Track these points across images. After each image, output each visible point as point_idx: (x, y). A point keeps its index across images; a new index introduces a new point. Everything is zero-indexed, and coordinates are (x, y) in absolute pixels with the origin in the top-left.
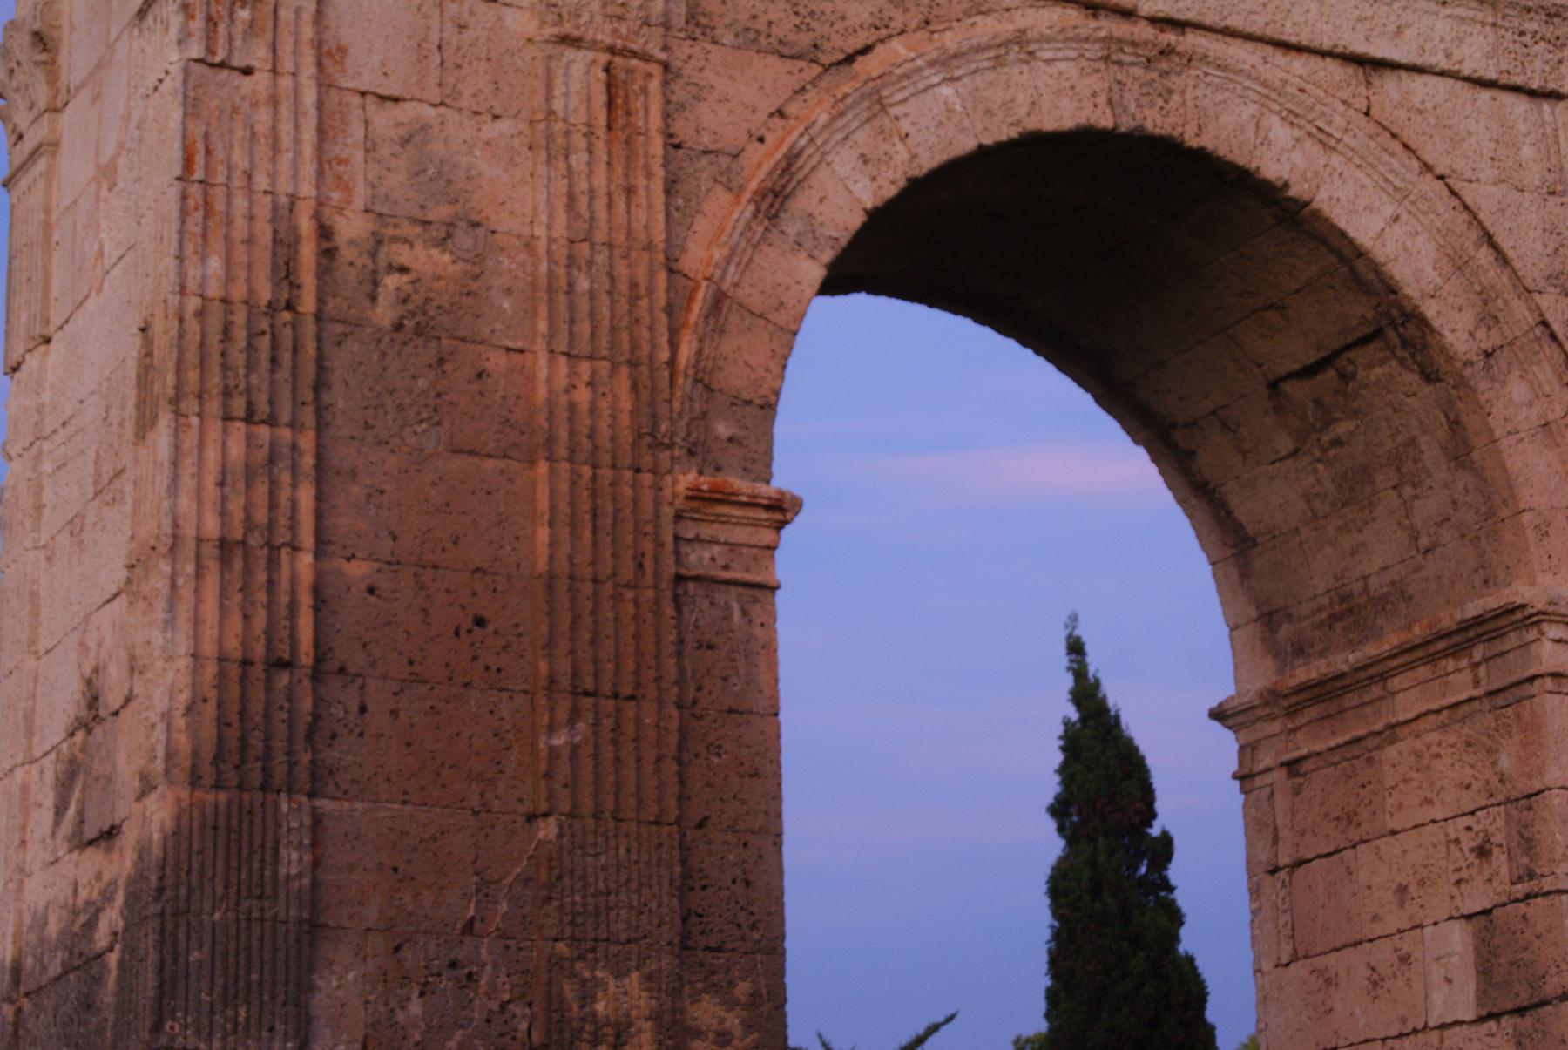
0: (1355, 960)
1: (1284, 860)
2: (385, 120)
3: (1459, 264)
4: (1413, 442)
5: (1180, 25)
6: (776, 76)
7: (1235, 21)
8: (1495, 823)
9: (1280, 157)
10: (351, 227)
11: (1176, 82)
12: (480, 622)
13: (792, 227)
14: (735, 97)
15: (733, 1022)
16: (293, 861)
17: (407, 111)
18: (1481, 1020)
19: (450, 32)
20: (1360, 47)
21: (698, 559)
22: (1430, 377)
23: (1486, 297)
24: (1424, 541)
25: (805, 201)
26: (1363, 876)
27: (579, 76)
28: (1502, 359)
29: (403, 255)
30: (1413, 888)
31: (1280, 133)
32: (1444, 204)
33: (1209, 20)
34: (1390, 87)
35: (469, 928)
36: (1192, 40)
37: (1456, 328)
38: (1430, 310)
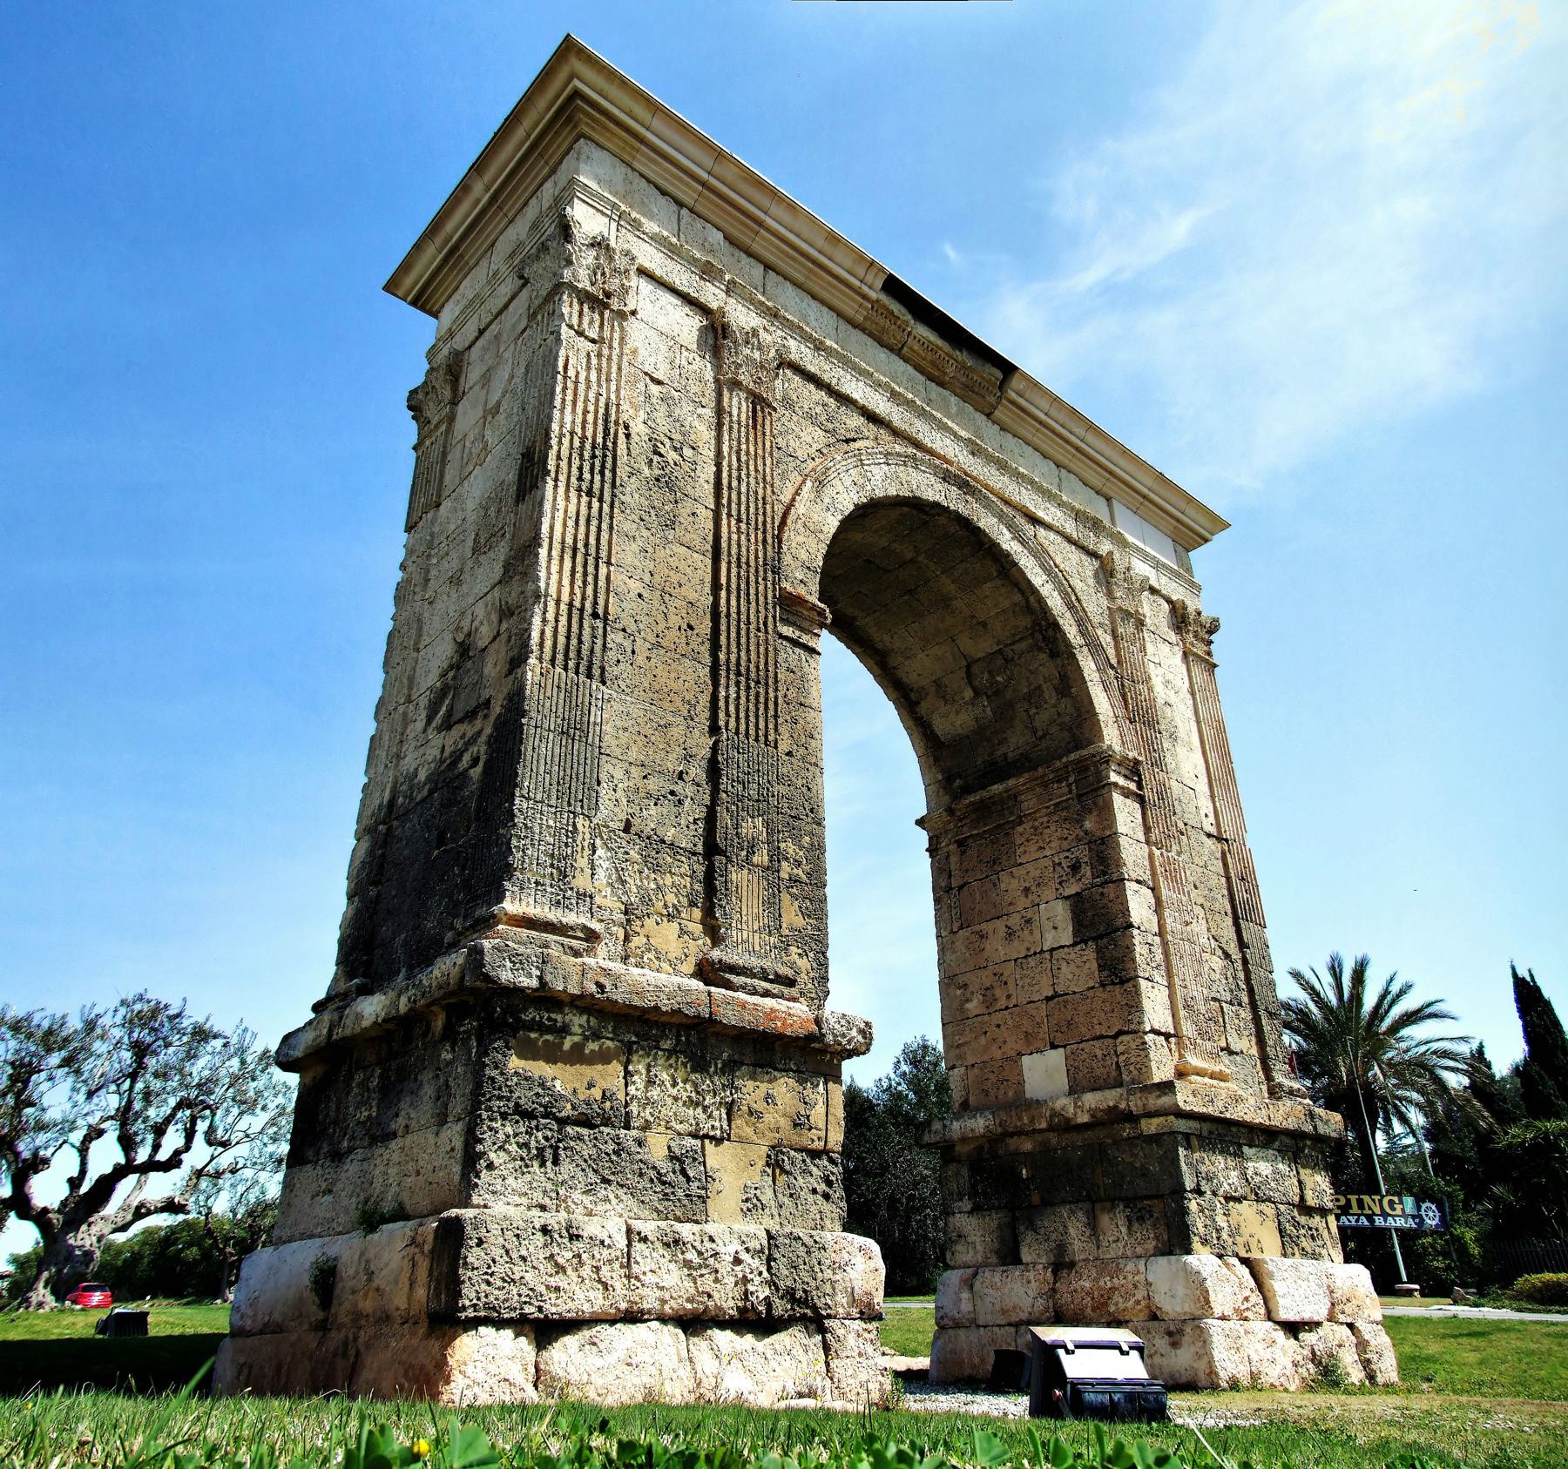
0: (1000, 925)
1: (955, 883)
4: (1039, 687)
8: (1082, 853)
12: (691, 627)
18: (1075, 944)
19: (684, 363)
22: (1054, 655)
24: (1040, 733)
26: (1003, 886)
30: (1033, 888)
35: (680, 776)
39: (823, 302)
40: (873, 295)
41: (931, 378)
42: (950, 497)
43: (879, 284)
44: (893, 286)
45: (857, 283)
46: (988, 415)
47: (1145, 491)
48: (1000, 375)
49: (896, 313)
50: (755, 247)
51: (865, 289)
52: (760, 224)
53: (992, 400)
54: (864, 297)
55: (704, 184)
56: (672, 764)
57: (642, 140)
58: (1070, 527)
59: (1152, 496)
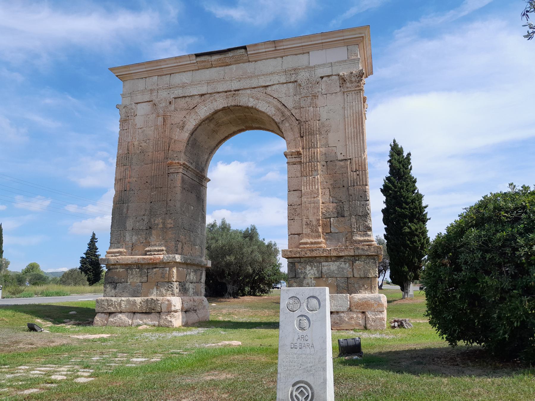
2: (140, 131)
3: (279, 109)
5: (238, 90)
6: (184, 113)
7: (245, 87)
9: (251, 103)
10: (136, 143)
11: (236, 98)
13: (185, 130)
14: (177, 118)
15: (172, 222)
16: (125, 210)
17: (142, 129)
20: (264, 84)
21: (171, 171)
23: (282, 113)
25: (186, 127)
27: (160, 119)
28: (285, 121)
29: (141, 144)
31: (251, 99)
32: (275, 102)
33: (242, 88)
34: (269, 88)
36: (240, 92)
37: (277, 119)
38: (273, 117)
39: (187, 71)
40: (195, 61)
41: (226, 66)
42: (231, 102)
43: (194, 57)
44: (197, 55)
45: (189, 62)
46: (249, 61)
47: (320, 41)
48: (243, 50)
49: (203, 60)
50: (165, 73)
51: (192, 62)
52: (162, 68)
53: (246, 58)
54: (194, 63)
55: (147, 71)
56: (142, 213)
57: (131, 73)
58: (283, 79)
59: (323, 41)
